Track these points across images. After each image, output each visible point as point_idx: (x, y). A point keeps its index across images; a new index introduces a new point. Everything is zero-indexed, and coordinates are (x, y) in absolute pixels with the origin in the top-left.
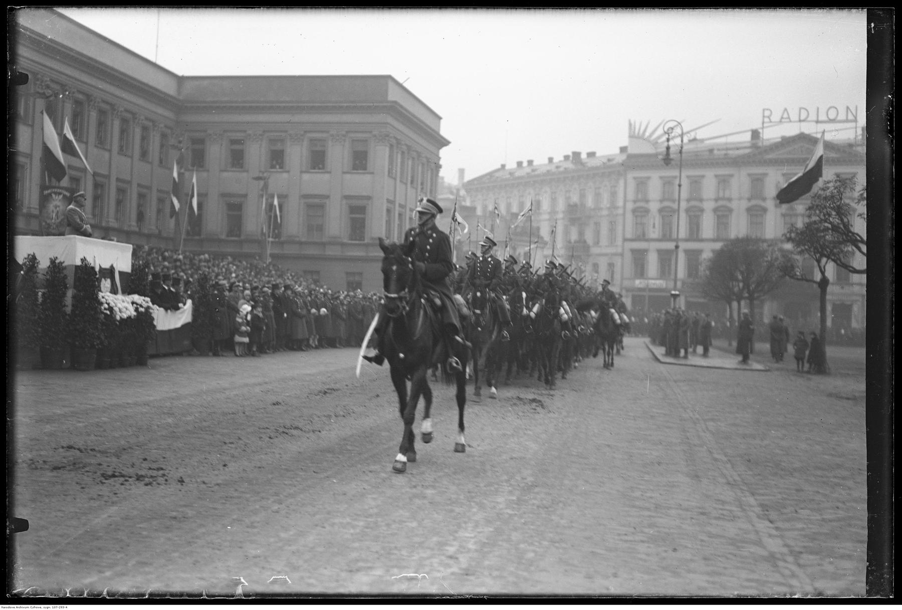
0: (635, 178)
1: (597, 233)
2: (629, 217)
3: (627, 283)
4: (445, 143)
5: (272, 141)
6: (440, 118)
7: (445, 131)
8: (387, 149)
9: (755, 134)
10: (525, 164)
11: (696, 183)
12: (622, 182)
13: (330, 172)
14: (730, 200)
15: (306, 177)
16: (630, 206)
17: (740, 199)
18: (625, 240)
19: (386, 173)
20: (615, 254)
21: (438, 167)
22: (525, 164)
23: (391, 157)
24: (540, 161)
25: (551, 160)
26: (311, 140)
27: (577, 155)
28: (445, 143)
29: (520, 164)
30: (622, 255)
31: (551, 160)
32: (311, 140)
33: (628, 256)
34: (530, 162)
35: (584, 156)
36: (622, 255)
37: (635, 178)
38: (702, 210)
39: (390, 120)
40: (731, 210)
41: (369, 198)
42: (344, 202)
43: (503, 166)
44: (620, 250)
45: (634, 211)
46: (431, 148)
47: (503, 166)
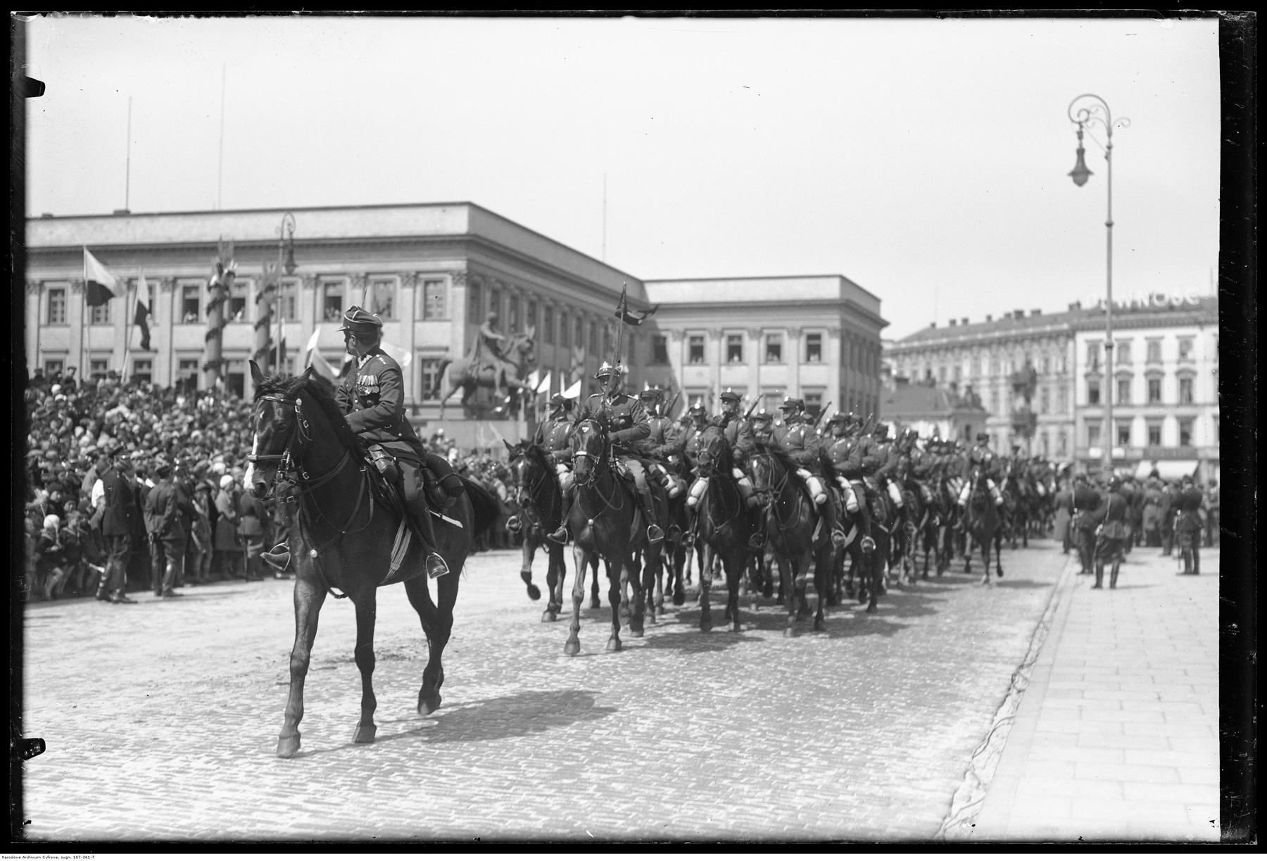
0: (1087, 341)
1: (1045, 399)
3: (1080, 454)
4: (884, 324)
5: (731, 338)
6: (878, 301)
7: (885, 314)
10: (959, 323)
11: (1154, 347)
12: (1071, 344)
14: (1193, 362)
15: (764, 369)
17: (1205, 360)
18: (1077, 407)
20: (1068, 422)
22: (959, 323)
24: (977, 318)
25: (989, 318)
26: (768, 337)
27: (1019, 314)
28: (884, 324)
29: (953, 322)
31: (989, 318)
32: (768, 337)
33: (1080, 423)
34: (965, 321)
35: (1027, 314)
36: (1074, 423)
37: (1087, 341)
38: (1162, 374)
40: (1195, 373)
41: (824, 387)
43: (933, 325)
44: (1071, 418)
46: (873, 330)
47: (933, 325)
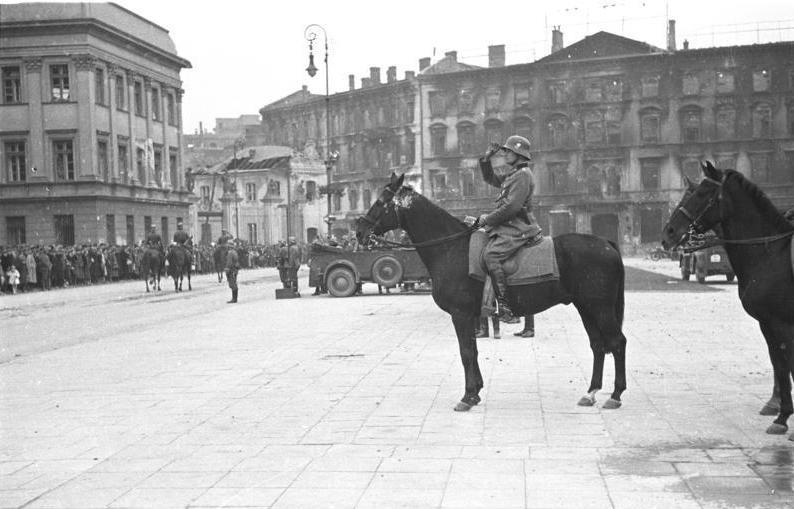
2: (427, 135)
7: (182, 53)
8: (91, 75)
9: (557, 35)
13: (27, 104)
16: (427, 123)
18: (424, 160)
19: (93, 100)
21: (179, 92)
23: (99, 83)
30: (421, 176)
39: (91, 40)
41: (75, 131)
42: (47, 137)
45: (431, 128)
46: (173, 74)
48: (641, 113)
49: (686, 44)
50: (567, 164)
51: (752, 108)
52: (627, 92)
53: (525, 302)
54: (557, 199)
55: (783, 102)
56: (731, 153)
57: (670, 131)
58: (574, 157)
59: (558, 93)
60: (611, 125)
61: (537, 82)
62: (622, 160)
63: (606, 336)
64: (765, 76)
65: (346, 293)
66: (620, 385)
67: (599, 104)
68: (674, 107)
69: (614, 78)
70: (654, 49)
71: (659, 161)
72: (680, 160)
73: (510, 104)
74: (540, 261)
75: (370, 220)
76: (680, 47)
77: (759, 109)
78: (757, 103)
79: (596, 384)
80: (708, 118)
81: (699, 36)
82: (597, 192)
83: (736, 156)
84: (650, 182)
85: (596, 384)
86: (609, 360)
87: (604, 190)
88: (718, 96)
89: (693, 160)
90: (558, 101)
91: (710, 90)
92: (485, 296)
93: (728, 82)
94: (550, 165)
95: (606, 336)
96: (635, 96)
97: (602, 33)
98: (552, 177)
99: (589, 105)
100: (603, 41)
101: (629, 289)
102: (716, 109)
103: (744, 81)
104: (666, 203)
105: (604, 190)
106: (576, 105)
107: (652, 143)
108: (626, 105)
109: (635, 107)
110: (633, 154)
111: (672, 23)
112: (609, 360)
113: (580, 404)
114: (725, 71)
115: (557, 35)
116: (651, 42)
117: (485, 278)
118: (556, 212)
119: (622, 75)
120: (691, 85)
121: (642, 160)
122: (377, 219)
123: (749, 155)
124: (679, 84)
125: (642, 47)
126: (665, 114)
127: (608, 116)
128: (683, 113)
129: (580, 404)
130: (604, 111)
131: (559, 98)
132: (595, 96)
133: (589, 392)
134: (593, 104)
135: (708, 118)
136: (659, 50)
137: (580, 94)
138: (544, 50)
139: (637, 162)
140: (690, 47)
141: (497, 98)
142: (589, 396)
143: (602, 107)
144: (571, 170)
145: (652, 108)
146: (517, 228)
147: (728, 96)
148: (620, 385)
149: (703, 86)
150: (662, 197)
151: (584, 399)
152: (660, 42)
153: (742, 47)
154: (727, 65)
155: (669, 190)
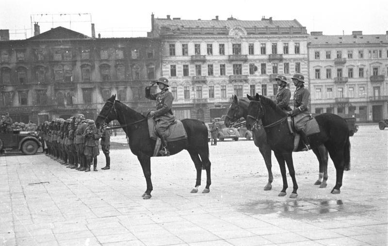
9: (37, 27)
48: (82, 67)
49: (99, 35)
50: (46, 90)
51: (132, 66)
52: (74, 56)
53: (173, 148)
54: (41, 108)
55: (145, 64)
56: (123, 87)
57: (96, 76)
58: (49, 87)
59: (39, 55)
60: (67, 72)
61: (29, 50)
62: (74, 89)
63: (202, 163)
64: (136, 52)
65: (33, 153)
66: (209, 183)
67: (61, 62)
68: (97, 66)
69: (67, 49)
70: (86, 37)
71: (91, 89)
72: (101, 89)
73: (14, 59)
74: (178, 131)
75: (103, 116)
76: (97, 37)
77: (135, 67)
78: (134, 64)
79: (198, 183)
80: (112, 70)
81: (105, 33)
82: (62, 104)
83: (126, 88)
84: (88, 99)
85: (198, 183)
86: (204, 173)
87: (65, 103)
88: (117, 60)
89: (107, 89)
90: (39, 59)
91: (113, 57)
92: (156, 147)
93: (120, 54)
94: (36, 90)
95: (202, 163)
96: (79, 58)
97: (60, 27)
98: (38, 96)
99: (55, 62)
100: (60, 32)
101: (112, 149)
102: (116, 66)
103: (127, 54)
104: (95, 109)
105: (65, 103)
106: (50, 62)
107: (88, 81)
108: (74, 63)
109: (79, 64)
110: (79, 86)
111: (93, 25)
112: (204, 173)
113: (192, 192)
114: (119, 49)
115: (37, 27)
116: (85, 34)
117: (156, 139)
118: (42, 114)
119: (72, 48)
120: (104, 54)
121: (84, 89)
122: (106, 116)
123: (131, 88)
124: (99, 56)
125: (82, 36)
126: (93, 67)
127: (66, 68)
128: (102, 67)
129: (192, 192)
130: (63, 65)
131: (40, 57)
132: (58, 57)
133: (196, 187)
134: (58, 62)
135: (112, 70)
136: (89, 37)
137: (52, 57)
138: (30, 34)
139: (81, 90)
140: (101, 37)
141: (7, 56)
142: (195, 188)
143: (62, 63)
144: (48, 93)
145: (88, 65)
146: (168, 117)
147: (121, 60)
148: (209, 183)
149: (109, 56)
150: (93, 107)
151: (194, 190)
152: (88, 33)
153: (126, 38)
154: (120, 46)
155: (96, 103)
